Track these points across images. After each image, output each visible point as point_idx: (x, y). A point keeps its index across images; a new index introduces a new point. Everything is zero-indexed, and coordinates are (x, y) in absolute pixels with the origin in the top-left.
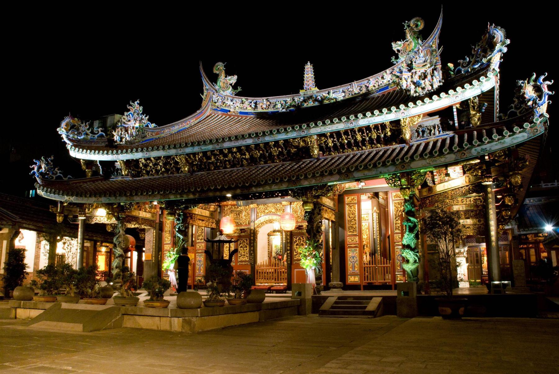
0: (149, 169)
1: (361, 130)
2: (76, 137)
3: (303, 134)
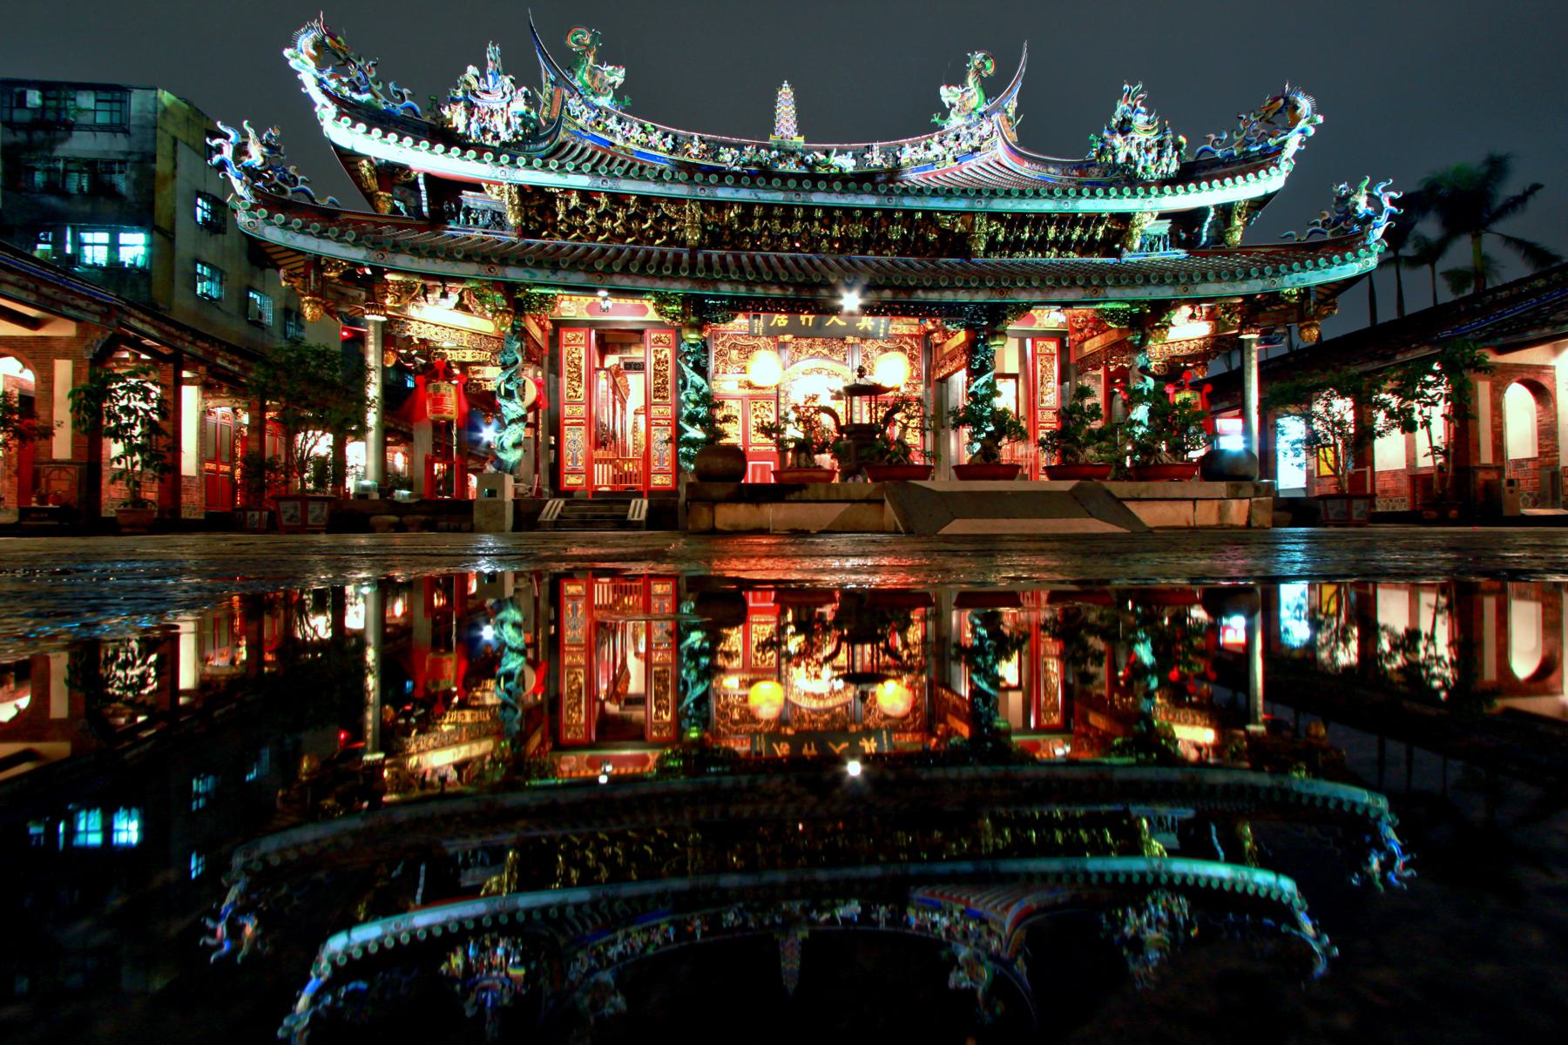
2: (346, 91)
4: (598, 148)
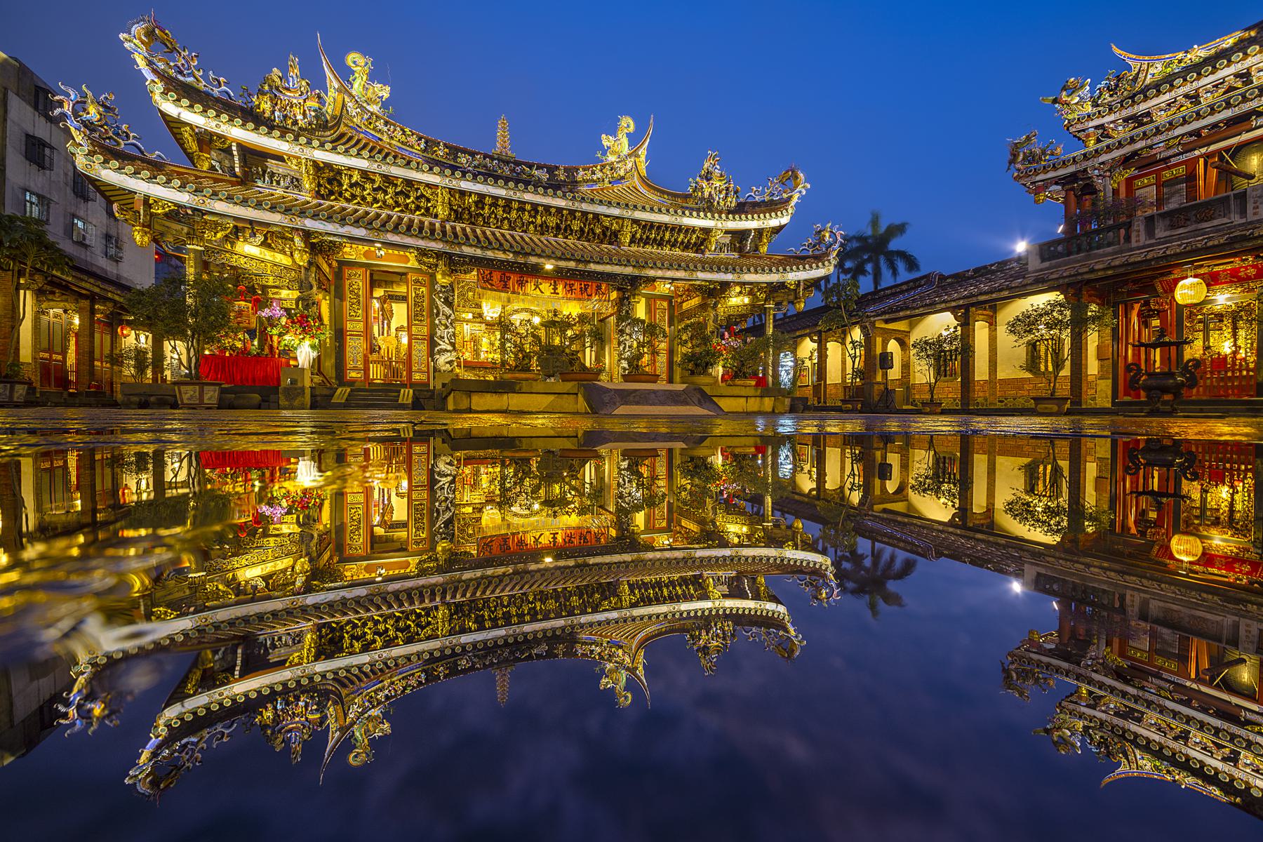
2: (172, 72)
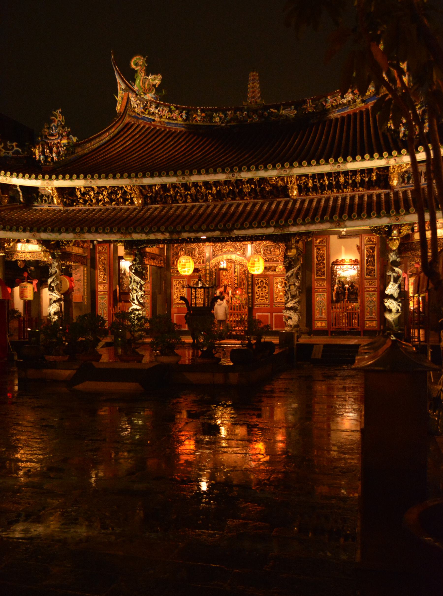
0: (87, 198)
1: (346, 173)
3: (283, 173)
4: (147, 124)
